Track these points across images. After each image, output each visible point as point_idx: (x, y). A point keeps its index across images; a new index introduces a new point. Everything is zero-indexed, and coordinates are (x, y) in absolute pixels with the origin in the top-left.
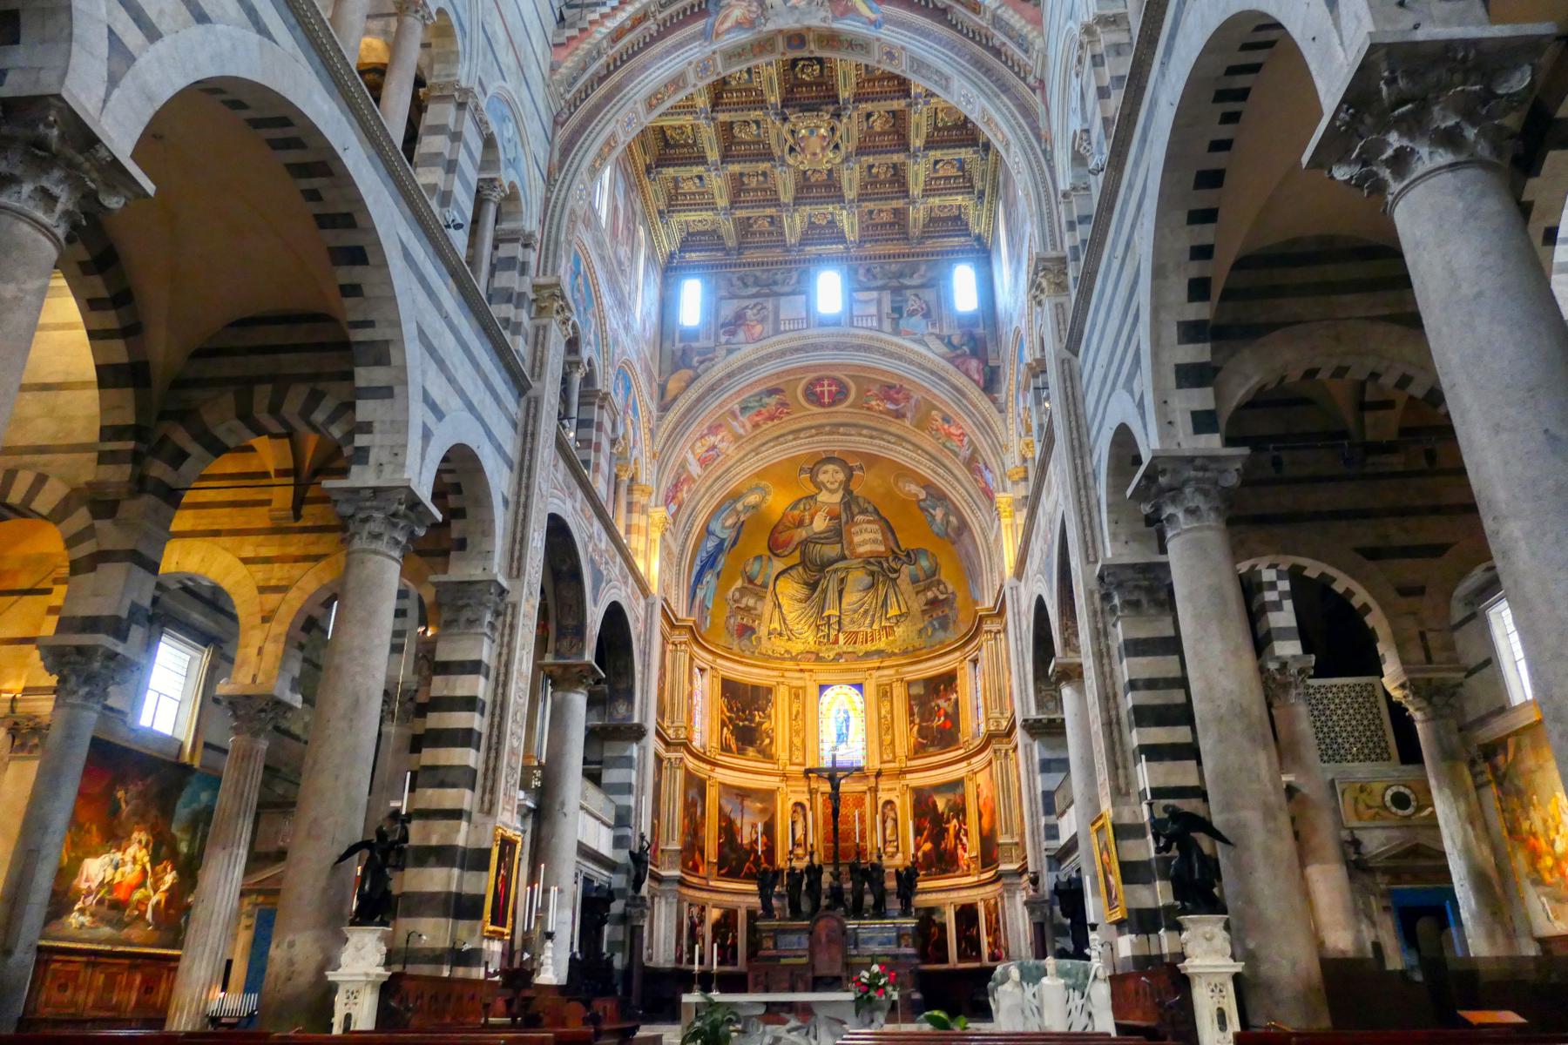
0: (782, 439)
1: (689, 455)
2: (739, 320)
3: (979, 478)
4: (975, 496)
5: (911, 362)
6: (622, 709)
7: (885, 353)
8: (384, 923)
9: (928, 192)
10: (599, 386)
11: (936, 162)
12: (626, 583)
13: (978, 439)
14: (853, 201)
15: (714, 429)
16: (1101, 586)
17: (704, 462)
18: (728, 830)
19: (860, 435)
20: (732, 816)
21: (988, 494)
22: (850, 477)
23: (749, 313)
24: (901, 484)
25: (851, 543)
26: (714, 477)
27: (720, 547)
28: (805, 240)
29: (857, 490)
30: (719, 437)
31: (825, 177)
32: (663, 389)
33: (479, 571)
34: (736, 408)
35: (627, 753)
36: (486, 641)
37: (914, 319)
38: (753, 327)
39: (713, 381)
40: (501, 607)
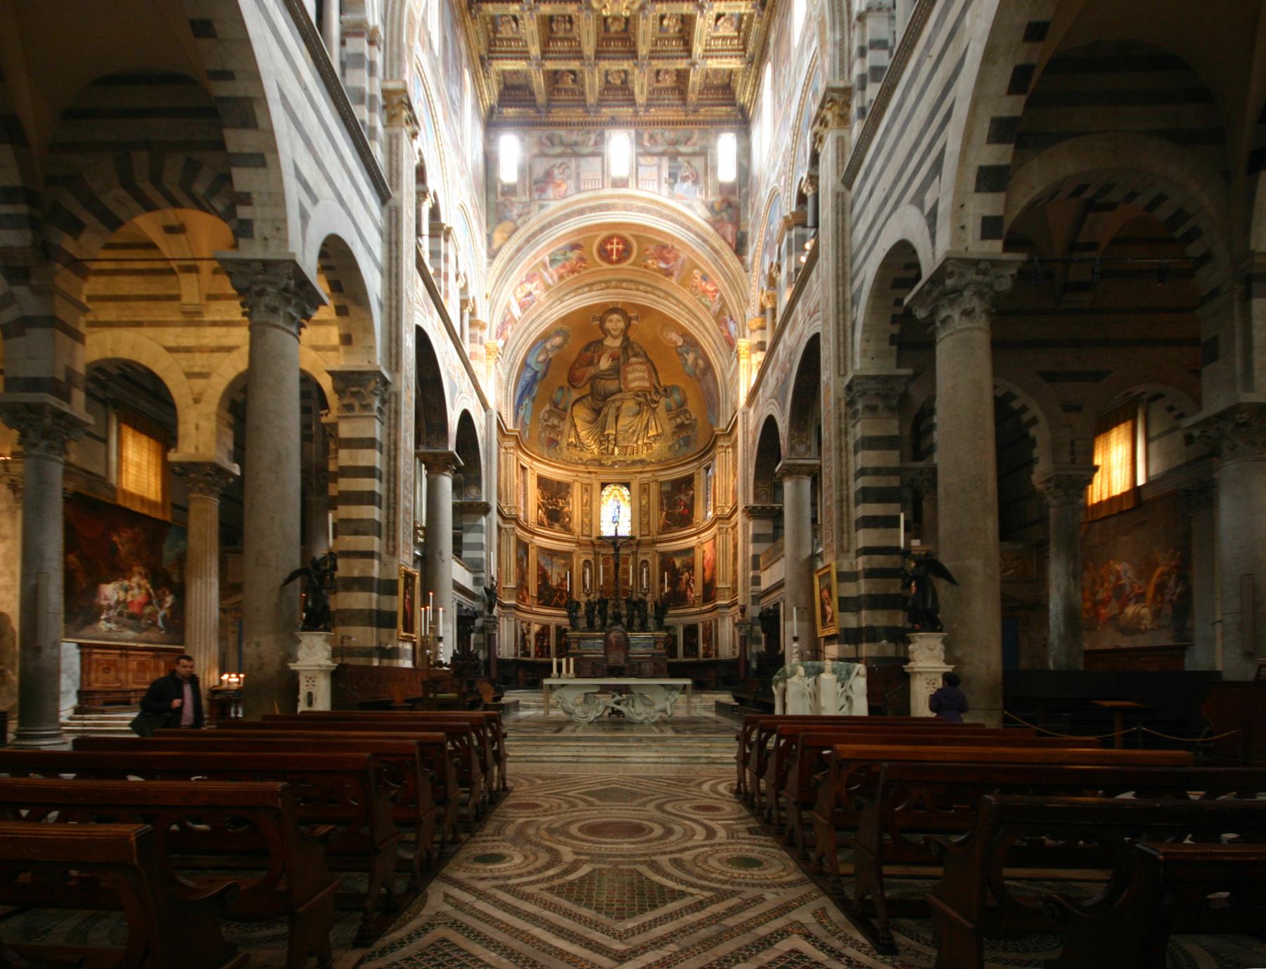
0: (580, 291)
1: (510, 296)
2: (548, 175)
3: (724, 328)
4: (718, 343)
8: (327, 629)
9: (708, 54)
11: (719, 17)
13: (727, 295)
14: (644, 58)
15: (530, 278)
16: (847, 395)
17: (523, 307)
21: (731, 343)
22: (628, 325)
23: (556, 171)
24: (665, 333)
25: (626, 379)
26: (530, 320)
27: (534, 377)
29: (633, 336)
30: (534, 285)
31: (623, 26)
33: (365, 363)
34: (547, 259)
36: (377, 423)
38: (559, 185)
40: (386, 396)
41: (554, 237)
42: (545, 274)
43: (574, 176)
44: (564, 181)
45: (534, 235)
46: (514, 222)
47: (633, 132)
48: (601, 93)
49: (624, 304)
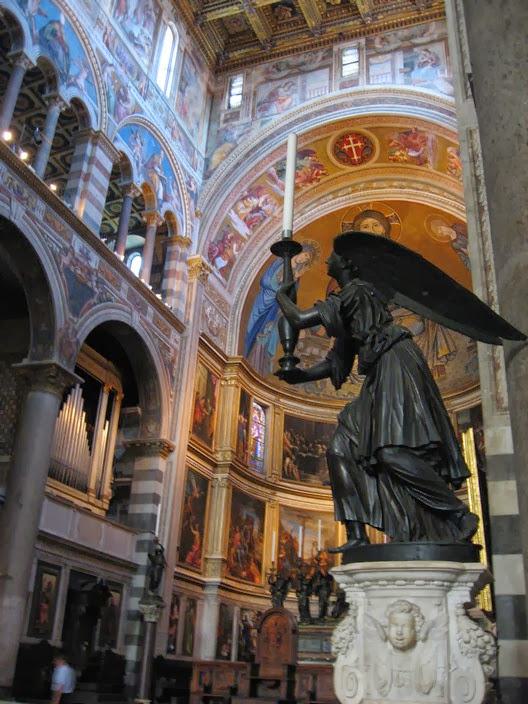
0: (323, 200)
5: (422, 105)
6: (152, 428)
7: (397, 101)
10: (95, 126)
12: (143, 310)
15: (255, 191)
17: (249, 223)
18: (288, 545)
19: (391, 187)
20: (293, 535)
23: (281, 90)
24: (433, 228)
26: (266, 237)
28: (323, 25)
30: (262, 199)
32: (207, 161)
34: (273, 170)
35: (154, 467)
37: (423, 70)
38: (284, 100)
39: (250, 148)
41: (276, 146)
42: (275, 186)
43: (299, 89)
44: (288, 96)
45: (255, 148)
46: (235, 142)
47: (363, 41)
48: (324, 16)
49: (374, 203)
